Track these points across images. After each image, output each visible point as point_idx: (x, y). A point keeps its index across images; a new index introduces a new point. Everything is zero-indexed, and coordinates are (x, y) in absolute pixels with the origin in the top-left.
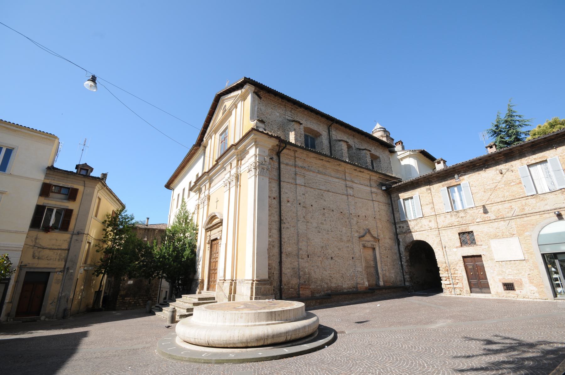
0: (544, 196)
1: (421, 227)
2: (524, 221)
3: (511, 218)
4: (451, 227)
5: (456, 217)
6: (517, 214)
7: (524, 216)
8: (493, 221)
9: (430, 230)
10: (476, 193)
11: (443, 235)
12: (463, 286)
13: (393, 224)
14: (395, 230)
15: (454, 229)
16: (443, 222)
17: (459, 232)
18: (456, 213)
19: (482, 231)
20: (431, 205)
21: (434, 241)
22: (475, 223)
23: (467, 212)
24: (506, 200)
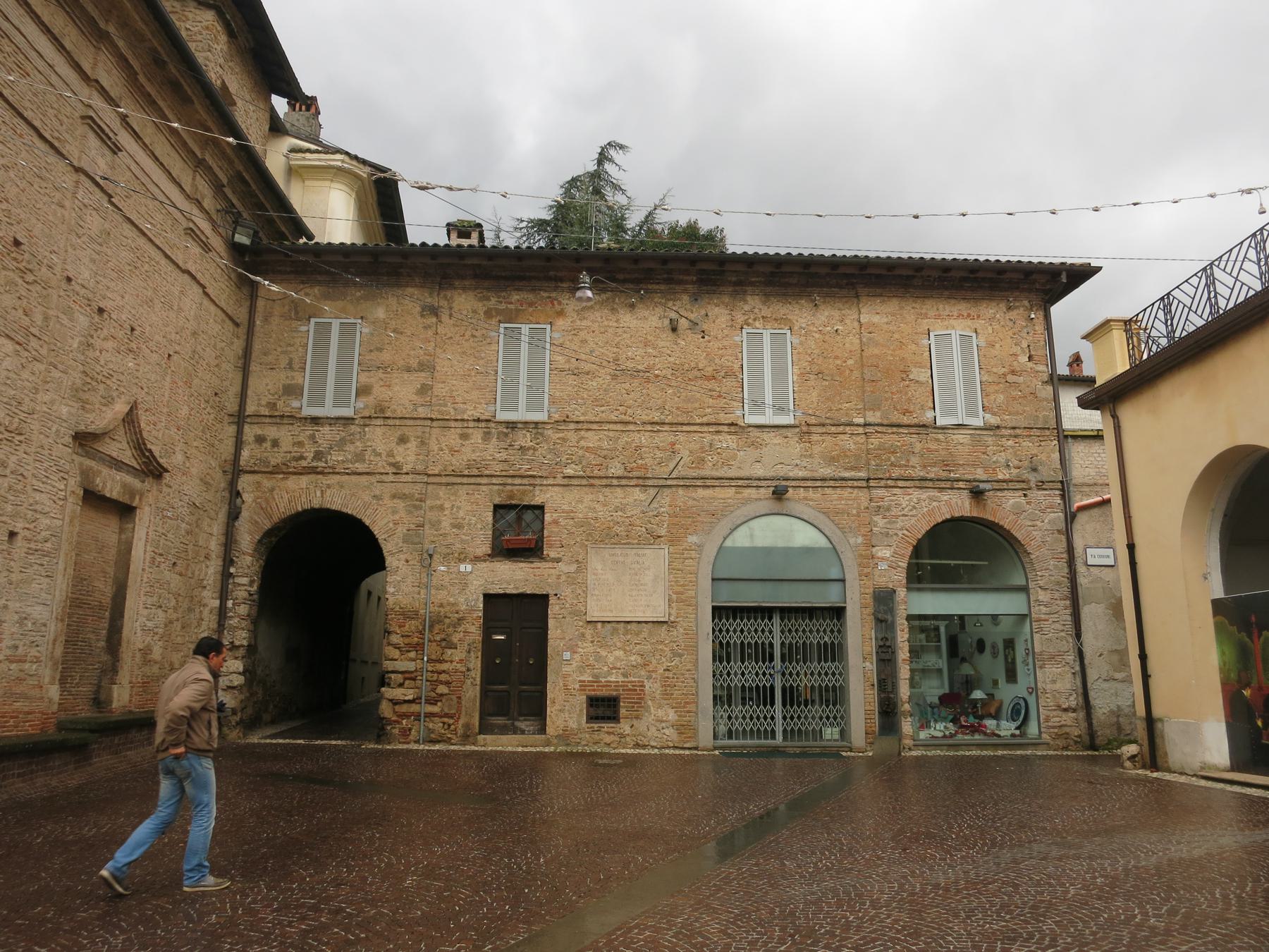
0: (758, 434)
1: (359, 457)
2: (694, 499)
3: (661, 482)
4: (472, 480)
5: (503, 445)
6: (683, 474)
7: (699, 483)
8: (615, 482)
9: (391, 478)
10: (588, 373)
11: (438, 502)
12: (459, 710)
13: (232, 419)
14: (232, 450)
15: (484, 488)
16: (453, 451)
17: (497, 501)
18: (505, 430)
19: (572, 512)
20: (423, 374)
21: (395, 524)
22: (559, 481)
23: (542, 434)
24: (667, 421)
